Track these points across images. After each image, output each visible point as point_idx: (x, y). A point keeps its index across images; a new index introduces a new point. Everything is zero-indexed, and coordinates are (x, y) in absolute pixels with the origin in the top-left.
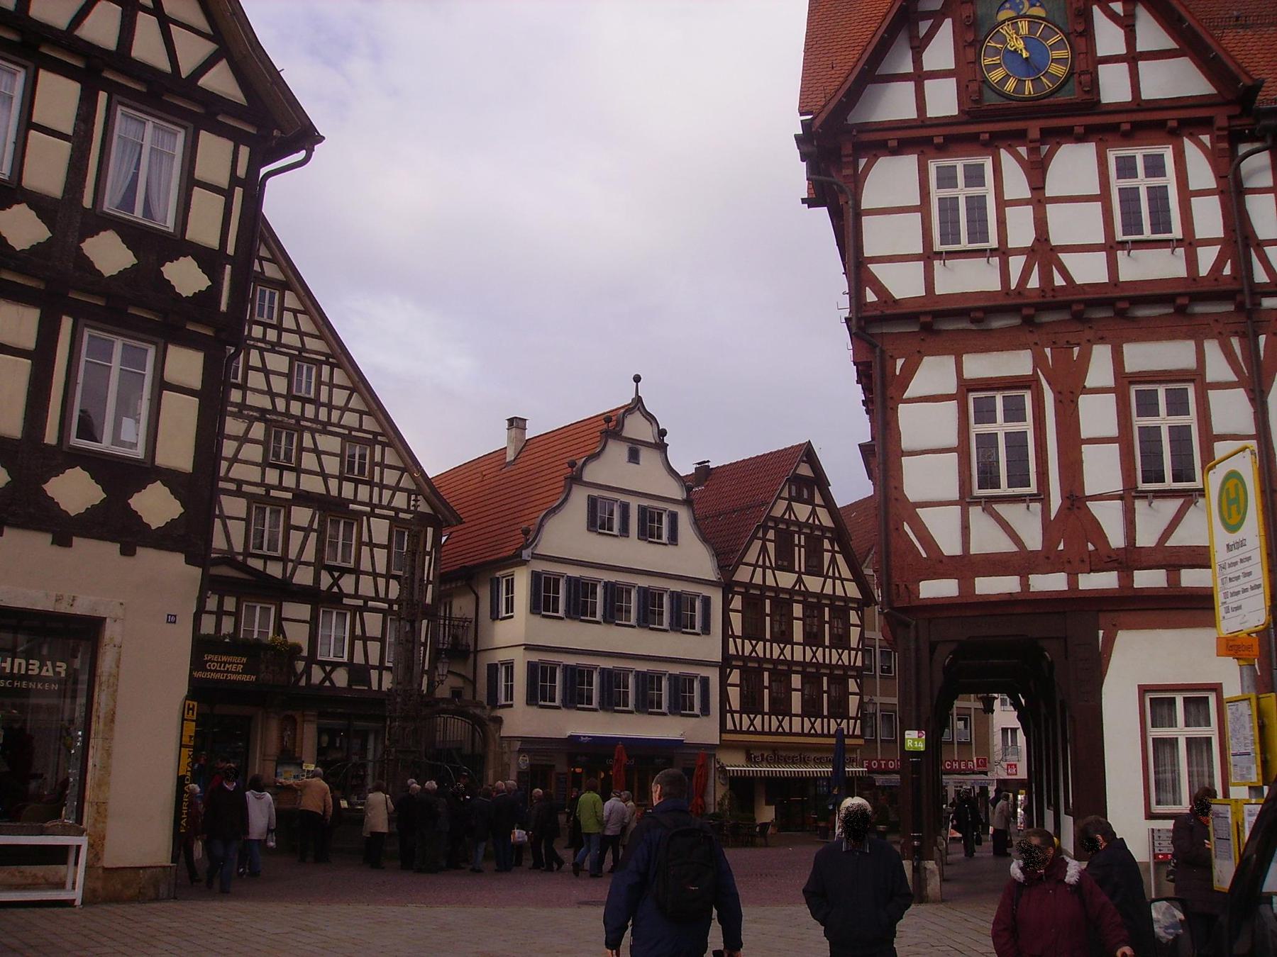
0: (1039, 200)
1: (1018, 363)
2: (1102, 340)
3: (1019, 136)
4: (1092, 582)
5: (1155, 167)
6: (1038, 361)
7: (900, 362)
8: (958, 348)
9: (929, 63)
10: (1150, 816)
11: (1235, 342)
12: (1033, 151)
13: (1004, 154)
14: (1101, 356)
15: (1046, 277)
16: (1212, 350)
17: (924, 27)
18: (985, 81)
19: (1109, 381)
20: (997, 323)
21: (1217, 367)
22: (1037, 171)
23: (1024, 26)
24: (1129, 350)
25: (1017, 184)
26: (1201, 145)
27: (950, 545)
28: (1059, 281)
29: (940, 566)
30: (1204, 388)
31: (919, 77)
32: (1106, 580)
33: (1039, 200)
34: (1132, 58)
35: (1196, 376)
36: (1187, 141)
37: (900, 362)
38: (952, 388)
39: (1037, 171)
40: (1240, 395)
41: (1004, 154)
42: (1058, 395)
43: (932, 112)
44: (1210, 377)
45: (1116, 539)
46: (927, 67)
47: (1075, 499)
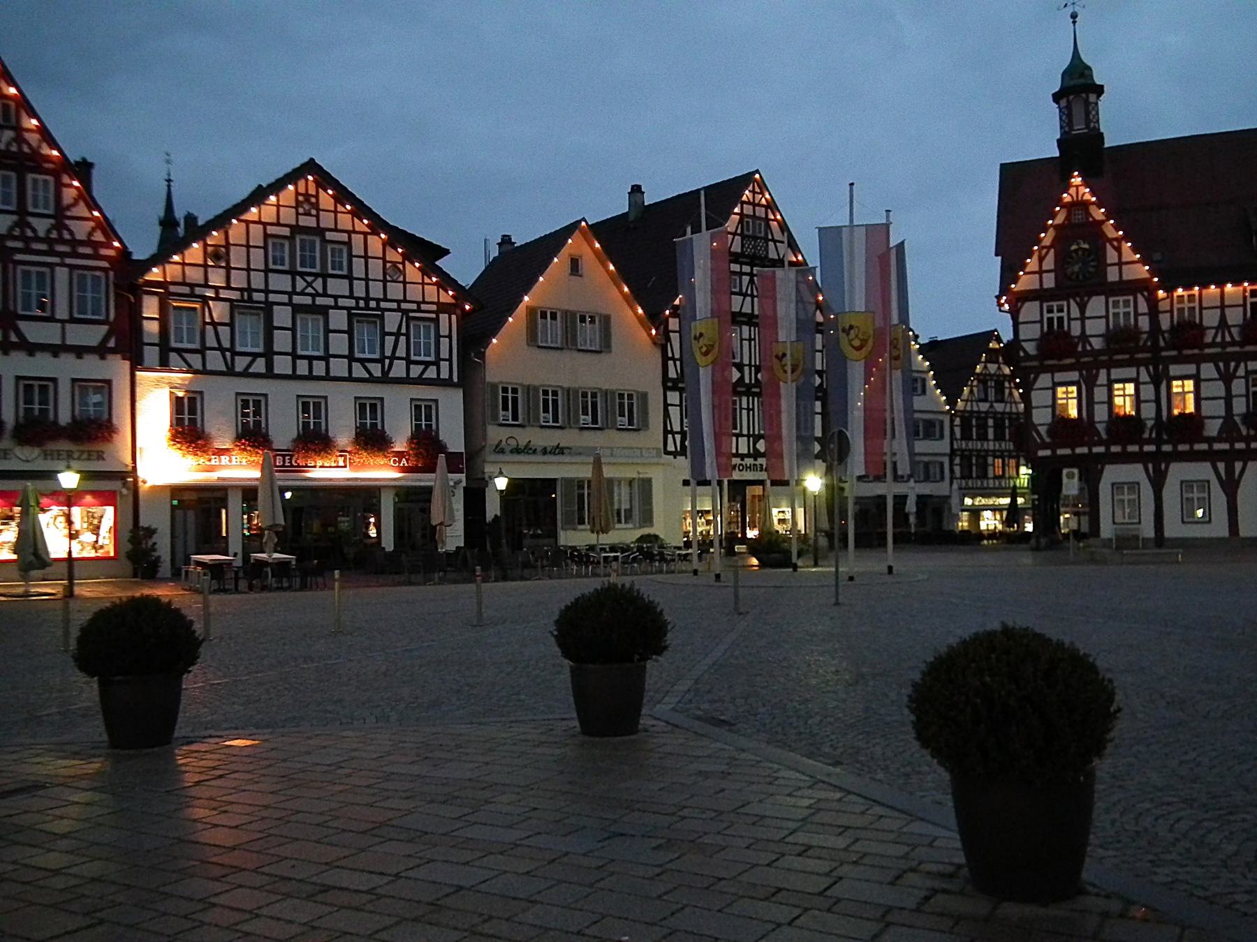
0: (1083, 319)
3: (1078, 294)
4: (1096, 450)
5: (1126, 304)
6: (1081, 375)
7: (1032, 376)
10: (1114, 523)
12: (1082, 299)
14: (1103, 373)
16: (1143, 370)
19: (1105, 382)
22: (1082, 308)
23: (1080, 253)
24: (1113, 371)
25: (1075, 312)
26: (1143, 296)
28: (1088, 348)
32: (1101, 449)
33: (1083, 319)
37: (1032, 376)
38: (1050, 385)
39: (1082, 308)
40: (1151, 387)
41: (1072, 301)
43: (1045, 286)
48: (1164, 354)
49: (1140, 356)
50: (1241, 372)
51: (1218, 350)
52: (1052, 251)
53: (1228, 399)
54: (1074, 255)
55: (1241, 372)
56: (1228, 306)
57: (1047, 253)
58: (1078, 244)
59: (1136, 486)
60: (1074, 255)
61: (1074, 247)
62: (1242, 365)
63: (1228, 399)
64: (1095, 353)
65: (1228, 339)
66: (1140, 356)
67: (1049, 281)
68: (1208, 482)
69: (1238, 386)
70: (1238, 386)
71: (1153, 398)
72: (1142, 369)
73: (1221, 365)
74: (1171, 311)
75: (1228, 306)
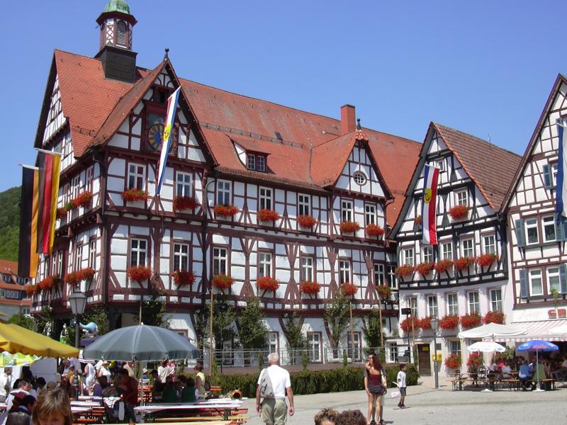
1: (145, 231)
2: (168, 228)
6: (151, 231)
7: (112, 225)
8: (130, 223)
9: (134, 132)
11: (201, 235)
13: (149, 166)
15: (157, 207)
17: (134, 118)
18: (149, 142)
20: (141, 217)
21: (196, 242)
27: (123, 285)
28: (160, 209)
29: (120, 291)
30: (192, 246)
31: (130, 135)
34: (187, 146)
35: (190, 242)
36: (196, 174)
37: (112, 225)
40: (200, 250)
41: (149, 166)
42: (155, 242)
44: (193, 244)
45: (167, 287)
46: (133, 133)
47: (157, 275)
48: (210, 225)
49: (193, 223)
50: (254, 248)
51: (242, 229)
52: (140, 119)
53: (247, 266)
54: (156, 128)
55: (254, 248)
56: (249, 198)
57: (136, 120)
58: (160, 121)
59: (185, 333)
60: (156, 128)
61: (156, 122)
62: (256, 242)
63: (247, 266)
64: (163, 215)
65: (248, 222)
66: (193, 223)
67: (136, 145)
68: (321, 333)
69: (253, 258)
70: (253, 258)
71: (202, 260)
72: (195, 235)
73: (244, 240)
74: (215, 192)
75: (249, 198)
